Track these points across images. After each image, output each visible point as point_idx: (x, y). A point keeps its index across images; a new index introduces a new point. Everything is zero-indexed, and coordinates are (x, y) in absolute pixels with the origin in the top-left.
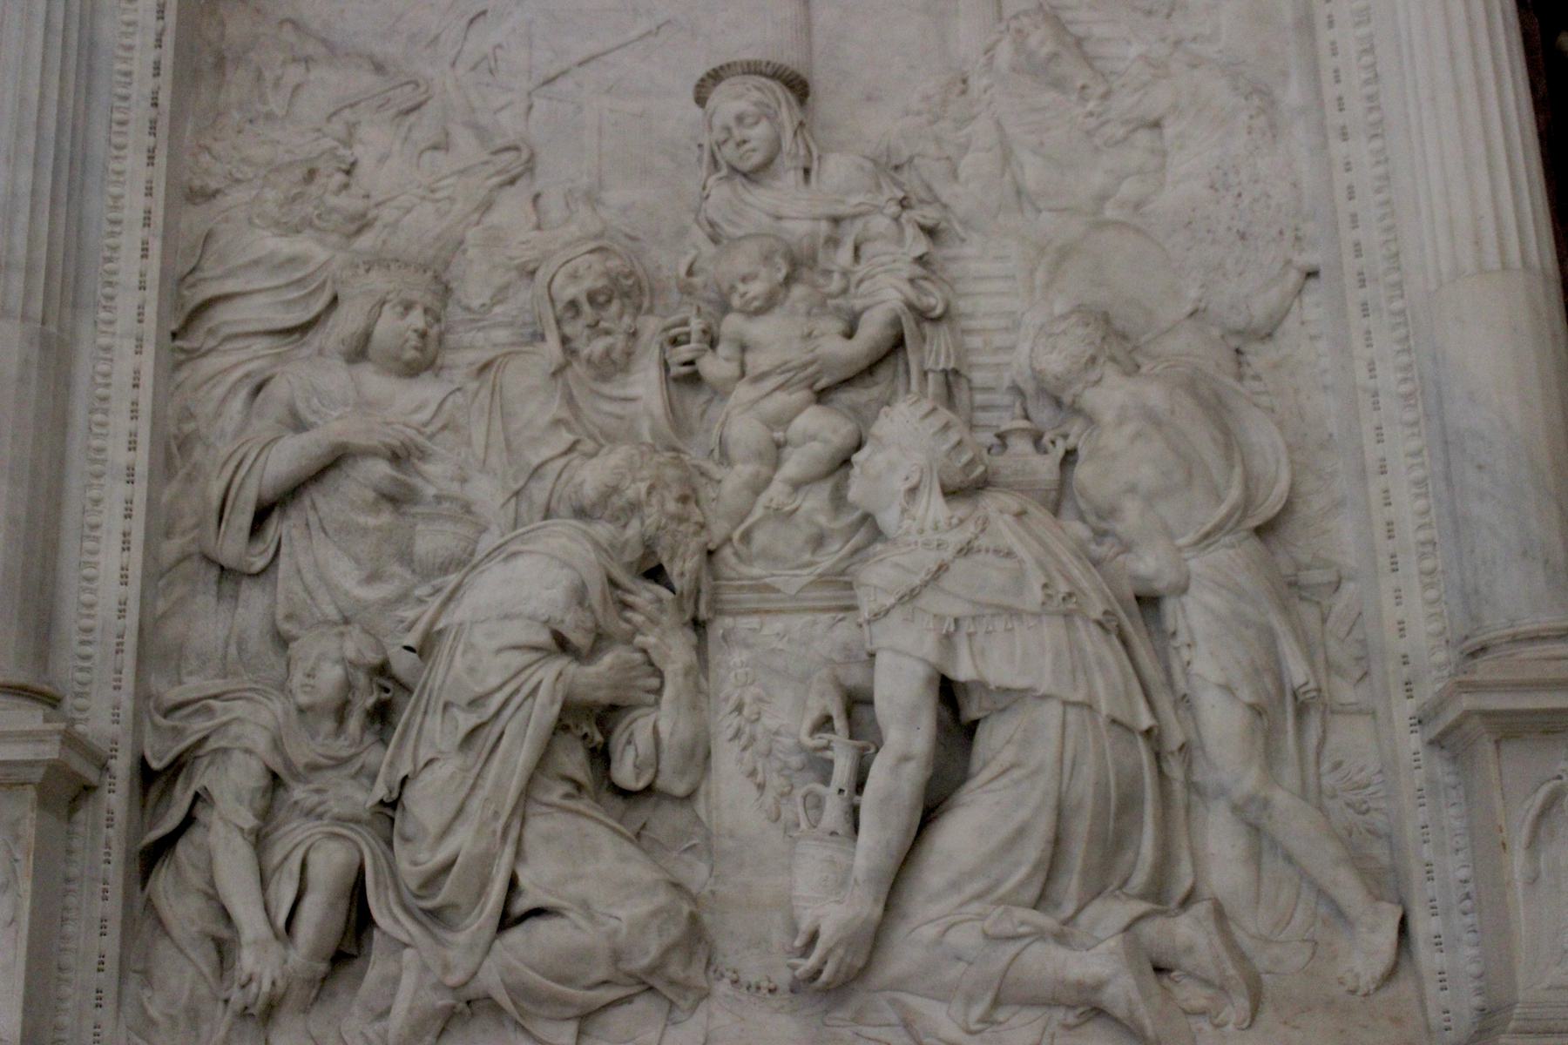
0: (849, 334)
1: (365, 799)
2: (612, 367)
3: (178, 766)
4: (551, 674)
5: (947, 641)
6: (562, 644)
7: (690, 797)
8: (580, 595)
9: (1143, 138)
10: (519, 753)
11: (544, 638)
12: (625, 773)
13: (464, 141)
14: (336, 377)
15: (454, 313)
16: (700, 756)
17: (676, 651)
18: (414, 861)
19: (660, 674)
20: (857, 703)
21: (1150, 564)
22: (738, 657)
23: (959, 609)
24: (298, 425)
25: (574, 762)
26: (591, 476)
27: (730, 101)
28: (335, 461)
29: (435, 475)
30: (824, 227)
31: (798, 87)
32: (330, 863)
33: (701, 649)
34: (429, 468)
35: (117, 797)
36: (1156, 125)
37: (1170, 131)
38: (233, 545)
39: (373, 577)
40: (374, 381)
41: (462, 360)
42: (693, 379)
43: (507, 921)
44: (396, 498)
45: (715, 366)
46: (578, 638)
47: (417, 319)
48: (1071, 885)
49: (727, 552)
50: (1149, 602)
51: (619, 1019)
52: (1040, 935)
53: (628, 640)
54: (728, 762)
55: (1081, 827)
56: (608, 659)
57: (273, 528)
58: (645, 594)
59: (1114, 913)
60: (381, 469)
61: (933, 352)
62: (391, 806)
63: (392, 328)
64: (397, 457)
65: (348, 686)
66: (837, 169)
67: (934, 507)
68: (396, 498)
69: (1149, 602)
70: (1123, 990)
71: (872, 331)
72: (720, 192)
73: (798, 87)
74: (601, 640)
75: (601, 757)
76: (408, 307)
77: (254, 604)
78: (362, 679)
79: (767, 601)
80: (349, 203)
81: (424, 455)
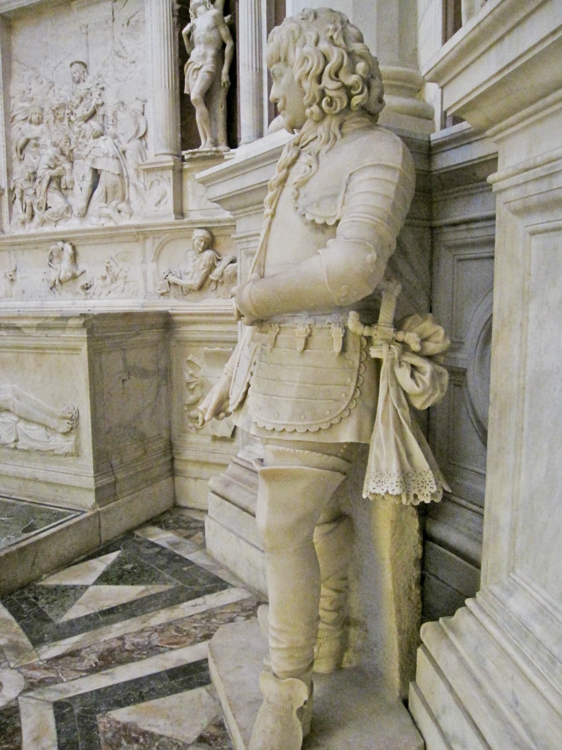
0: (87, 110)
5: (93, 161)
6: (50, 168)
7: (72, 189)
8: (51, 160)
9: (133, 65)
11: (47, 167)
12: (63, 186)
13: (45, 81)
15: (45, 113)
16: (73, 182)
17: (67, 166)
19: (65, 170)
21: (124, 145)
22: (77, 166)
23: (93, 157)
25: (54, 185)
29: (41, 142)
30: (86, 91)
31: (85, 65)
33: (72, 166)
34: (41, 140)
36: (134, 62)
37: (136, 62)
39: (35, 158)
40: (33, 127)
41: (45, 121)
43: (46, 209)
44: (36, 145)
46: (52, 166)
47: (37, 115)
48: (109, 199)
49: (74, 150)
50: (124, 152)
51: (60, 222)
52: (105, 207)
53: (60, 165)
55: (109, 191)
56: (59, 168)
57: (24, 152)
58: (62, 158)
60: (34, 141)
64: (36, 139)
65: (29, 176)
68: (36, 145)
71: (91, 109)
72: (74, 85)
74: (56, 166)
75: (59, 184)
76: (36, 114)
78: (31, 175)
80: (30, 96)
81: (40, 138)
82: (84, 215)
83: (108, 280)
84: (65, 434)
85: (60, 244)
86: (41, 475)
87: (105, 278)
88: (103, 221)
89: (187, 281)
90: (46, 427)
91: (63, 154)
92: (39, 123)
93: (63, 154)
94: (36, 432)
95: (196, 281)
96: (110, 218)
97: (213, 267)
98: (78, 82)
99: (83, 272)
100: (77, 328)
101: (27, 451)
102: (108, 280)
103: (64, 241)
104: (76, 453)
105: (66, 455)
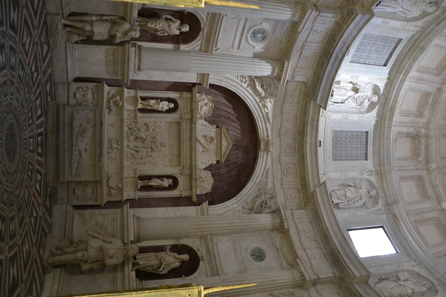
1: (136, 129)
2: (153, 139)
3: (137, 123)
4: (140, 137)
10: (136, 135)
14: (153, 128)
16: (137, 142)
17: (141, 141)
18: (133, 131)
20: (139, 148)
21: (144, 159)
24: (151, 126)
26: (148, 138)
27: (164, 144)
28: (149, 128)
32: (133, 129)
35: (136, 120)
38: (146, 124)
42: (152, 142)
44: (147, 130)
45: (152, 143)
50: (142, 159)
54: (137, 143)
59: (130, 157)
61: (153, 151)
62: (135, 130)
63: (154, 130)
64: (149, 131)
66: (161, 147)
67: (145, 151)
68: (147, 130)
69: (142, 159)
70: (127, 157)
71: (153, 149)
73: (165, 146)
74: (141, 138)
75: (137, 138)
77: (143, 125)
79: (143, 144)
82: (128, 146)
83: (111, 159)
84: (76, 174)
85: (120, 145)
86: (66, 166)
87: (111, 158)
88: (126, 153)
89: (110, 182)
90: (77, 168)
91: (144, 140)
92: (153, 131)
93: (144, 140)
94: (76, 165)
95: (110, 185)
96: (127, 155)
97: (113, 189)
98: (161, 145)
99: (113, 151)
100: (99, 179)
101: (71, 162)
102: (111, 159)
103: (121, 146)
104: (71, 175)
105: (71, 174)
